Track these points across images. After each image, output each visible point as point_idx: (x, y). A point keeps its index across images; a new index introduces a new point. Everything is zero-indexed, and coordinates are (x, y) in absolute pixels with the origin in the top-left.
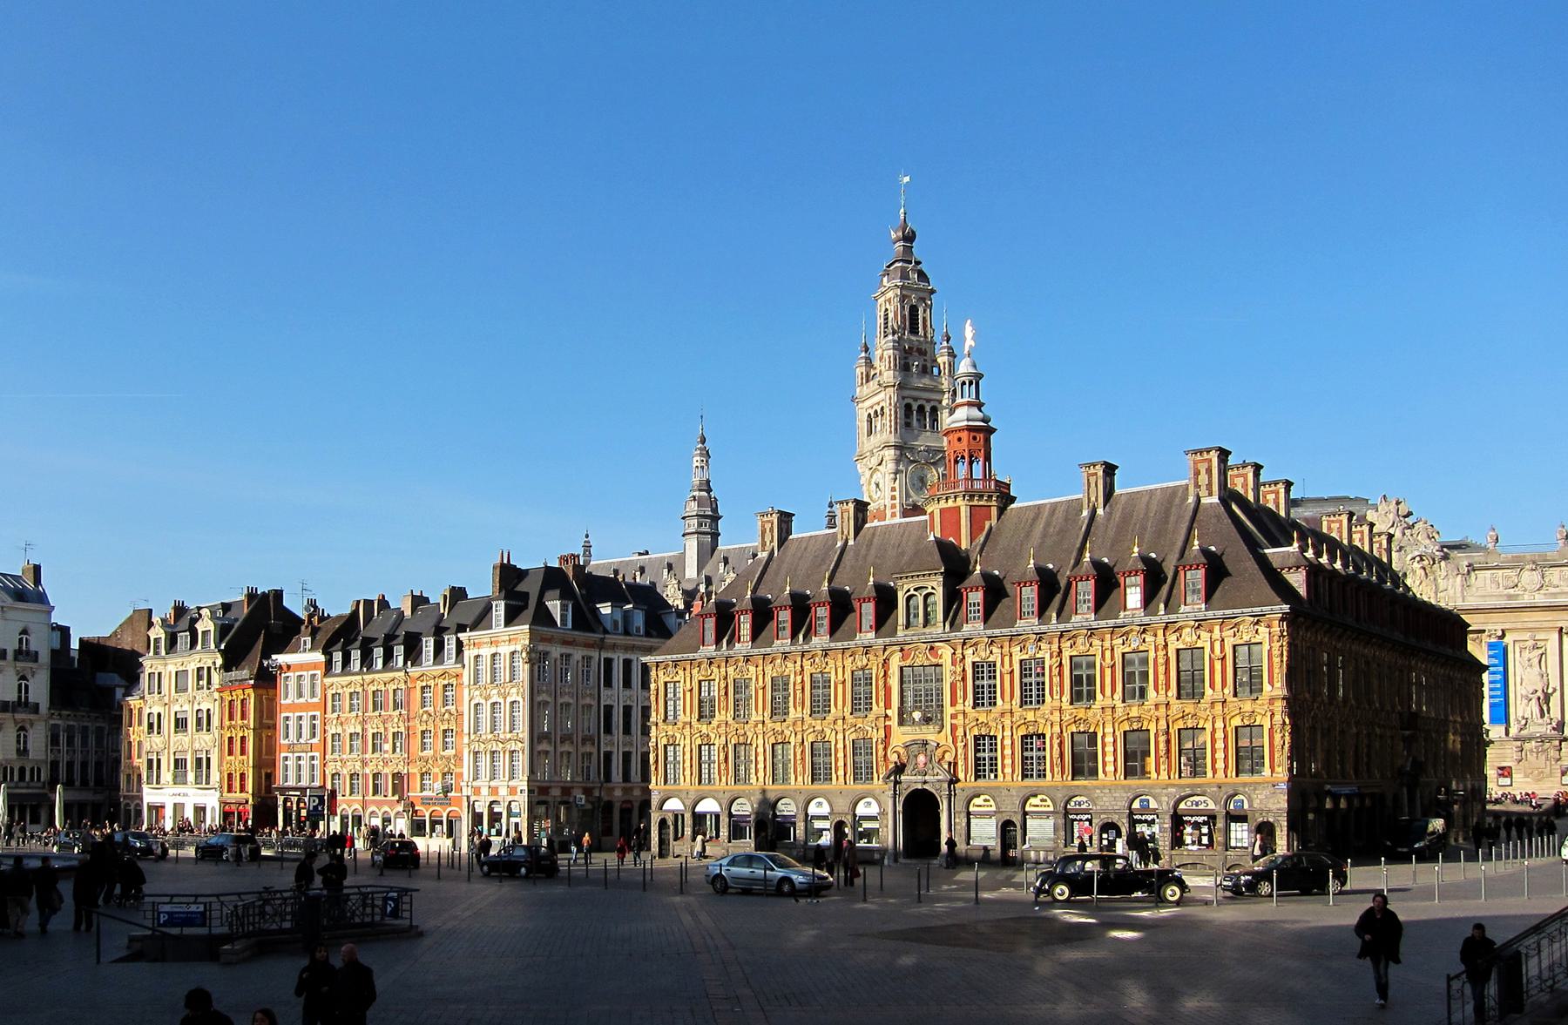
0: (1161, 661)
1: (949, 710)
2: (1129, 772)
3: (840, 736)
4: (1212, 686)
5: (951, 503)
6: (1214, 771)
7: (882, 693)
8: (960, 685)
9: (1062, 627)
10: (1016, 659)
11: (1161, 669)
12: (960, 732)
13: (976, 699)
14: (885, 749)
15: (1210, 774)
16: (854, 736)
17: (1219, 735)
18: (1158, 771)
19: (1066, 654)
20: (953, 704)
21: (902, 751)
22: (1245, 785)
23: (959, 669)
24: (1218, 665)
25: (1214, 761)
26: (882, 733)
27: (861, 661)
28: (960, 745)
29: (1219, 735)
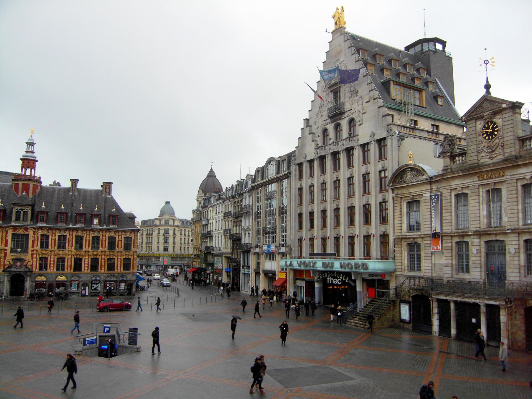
0: (104, 239)
1: (30, 248)
2: (92, 269)
4: (118, 247)
6: (117, 269)
7: (4, 242)
10: (57, 235)
11: (104, 242)
12: (35, 256)
13: (41, 246)
15: (116, 270)
17: (119, 260)
18: (101, 269)
19: (74, 235)
20: (33, 246)
21: (11, 261)
22: (125, 273)
23: (36, 236)
25: (117, 267)
28: (35, 260)
29: (119, 260)
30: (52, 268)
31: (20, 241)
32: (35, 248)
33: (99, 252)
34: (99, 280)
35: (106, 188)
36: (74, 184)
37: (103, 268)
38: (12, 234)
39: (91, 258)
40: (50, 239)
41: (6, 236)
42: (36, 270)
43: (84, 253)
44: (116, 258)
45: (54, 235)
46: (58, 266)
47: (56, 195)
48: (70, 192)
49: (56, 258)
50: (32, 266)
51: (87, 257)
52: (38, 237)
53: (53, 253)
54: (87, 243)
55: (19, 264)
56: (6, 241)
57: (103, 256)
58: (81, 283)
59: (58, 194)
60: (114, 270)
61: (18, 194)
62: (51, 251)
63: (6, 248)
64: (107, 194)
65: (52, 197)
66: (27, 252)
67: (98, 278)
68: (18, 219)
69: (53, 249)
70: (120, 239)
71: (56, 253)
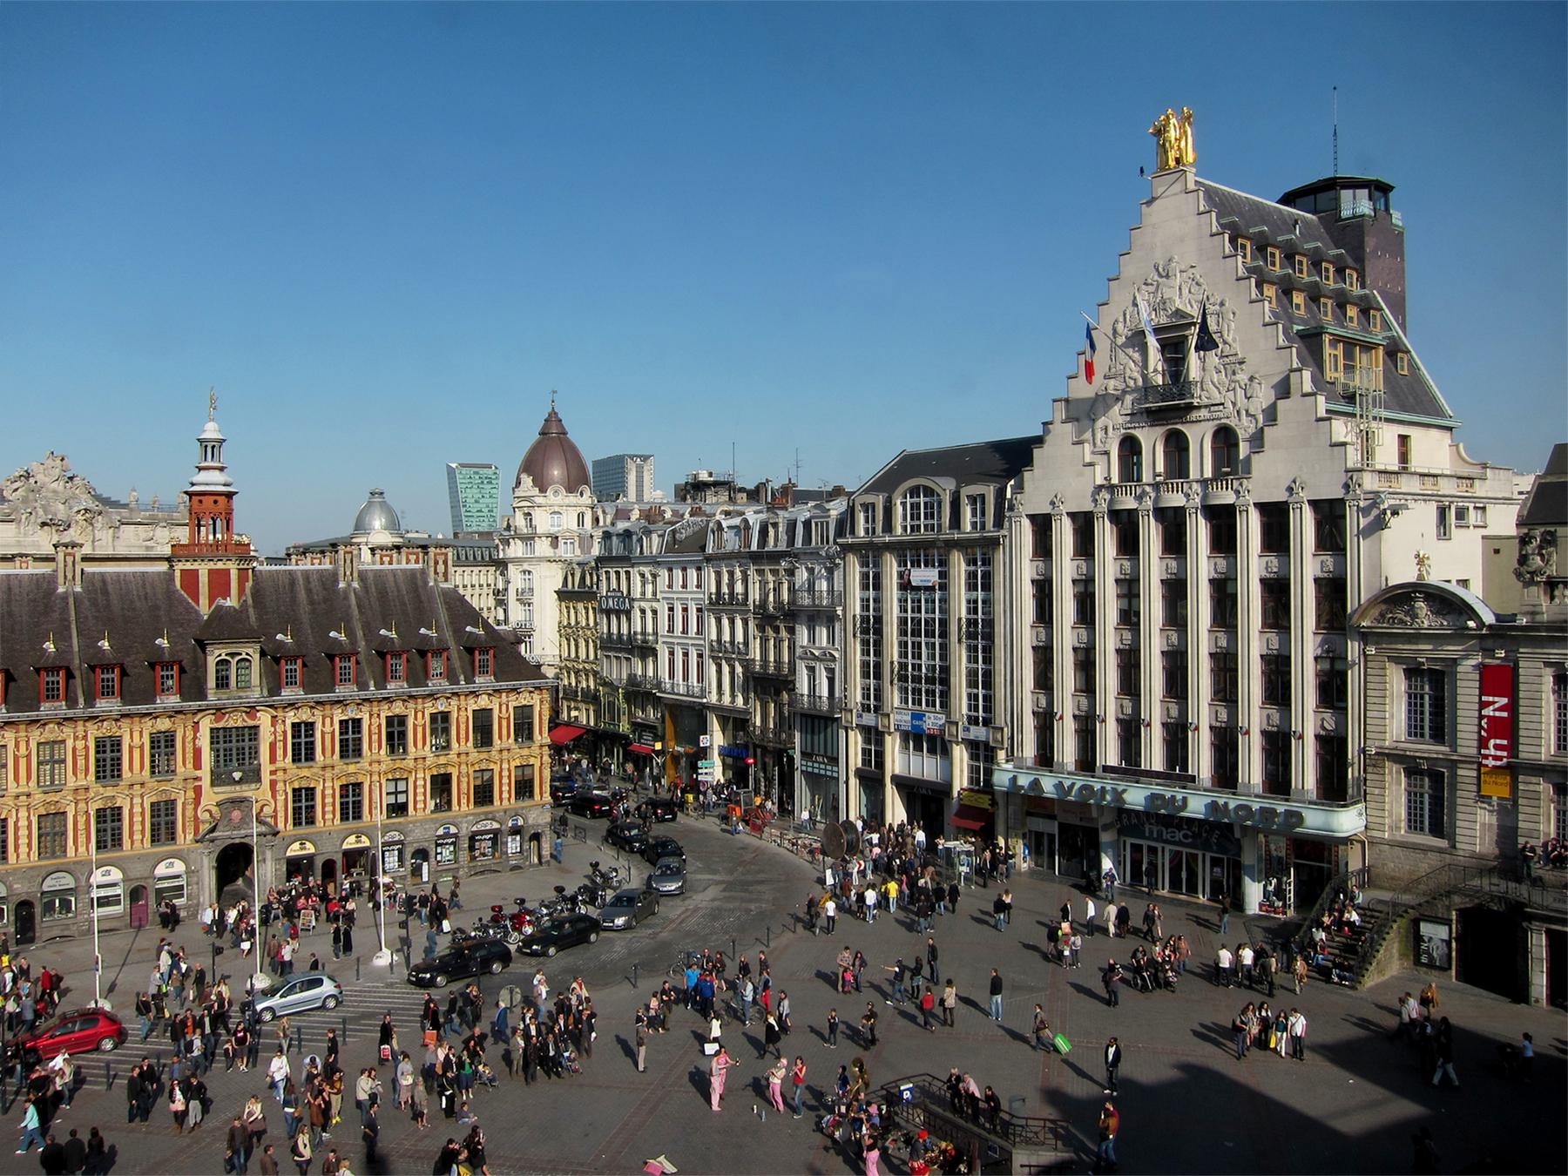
3: (137, 800)
5: (220, 565)
7: (190, 756)
8: (280, 745)
9: (384, 693)
11: (463, 726)
12: (280, 786)
14: (196, 809)
15: (497, 802)
16: (154, 799)
20: (273, 760)
21: (215, 810)
24: (504, 723)
25: (501, 792)
26: (191, 794)
27: (164, 724)
28: (281, 798)
30: (329, 816)
31: (235, 751)
32: (280, 764)
33: (453, 756)
34: (456, 836)
35: (436, 563)
36: (348, 557)
37: (464, 801)
38: (212, 730)
39: (432, 776)
40: (318, 735)
41: (195, 738)
42: (285, 825)
43: (411, 764)
44: (496, 768)
45: (328, 721)
46: (344, 806)
47: (302, 595)
48: (336, 581)
49: (337, 785)
50: (275, 817)
51: (420, 775)
52: (285, 732)
53: (328, 775)
54: (420, 736)
55: (236, 814)
56: (197, 753)
57: (463, 767)
58: (409, 851)
59: (309, 591)
60: (491, 802)
61: (197, 602)
62: (324, 768)
63: (198, 773)
64: (441, 578)
65: (294, 600)
66: (259, 780)
67: (453, 830)
68: (223, 682)
69: (329, 761)
70: (504, 714)
71: (336, 770)
